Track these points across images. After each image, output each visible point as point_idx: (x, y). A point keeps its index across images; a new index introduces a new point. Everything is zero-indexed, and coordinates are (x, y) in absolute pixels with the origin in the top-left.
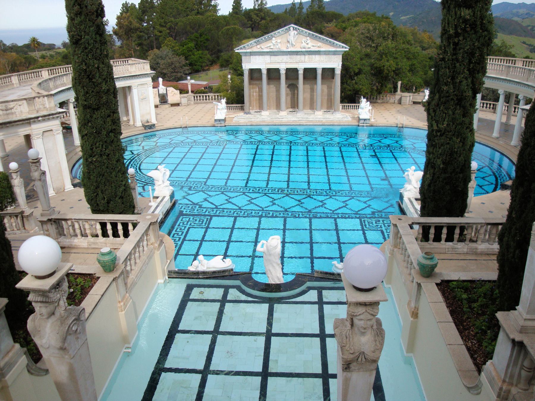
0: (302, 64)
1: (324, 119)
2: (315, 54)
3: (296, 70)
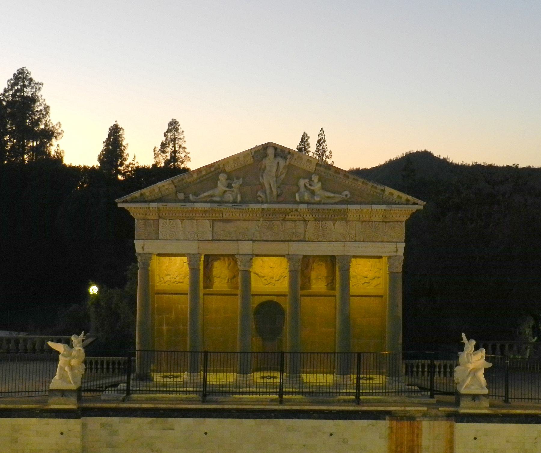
2: (334, 221)
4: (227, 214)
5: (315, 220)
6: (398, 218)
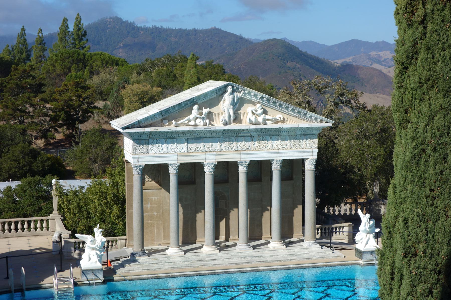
0: (244, 154)
1: (292, 255)
3: (234, 165)
4: (199, 134)
5: (259, 136)
6: (314, 132)
